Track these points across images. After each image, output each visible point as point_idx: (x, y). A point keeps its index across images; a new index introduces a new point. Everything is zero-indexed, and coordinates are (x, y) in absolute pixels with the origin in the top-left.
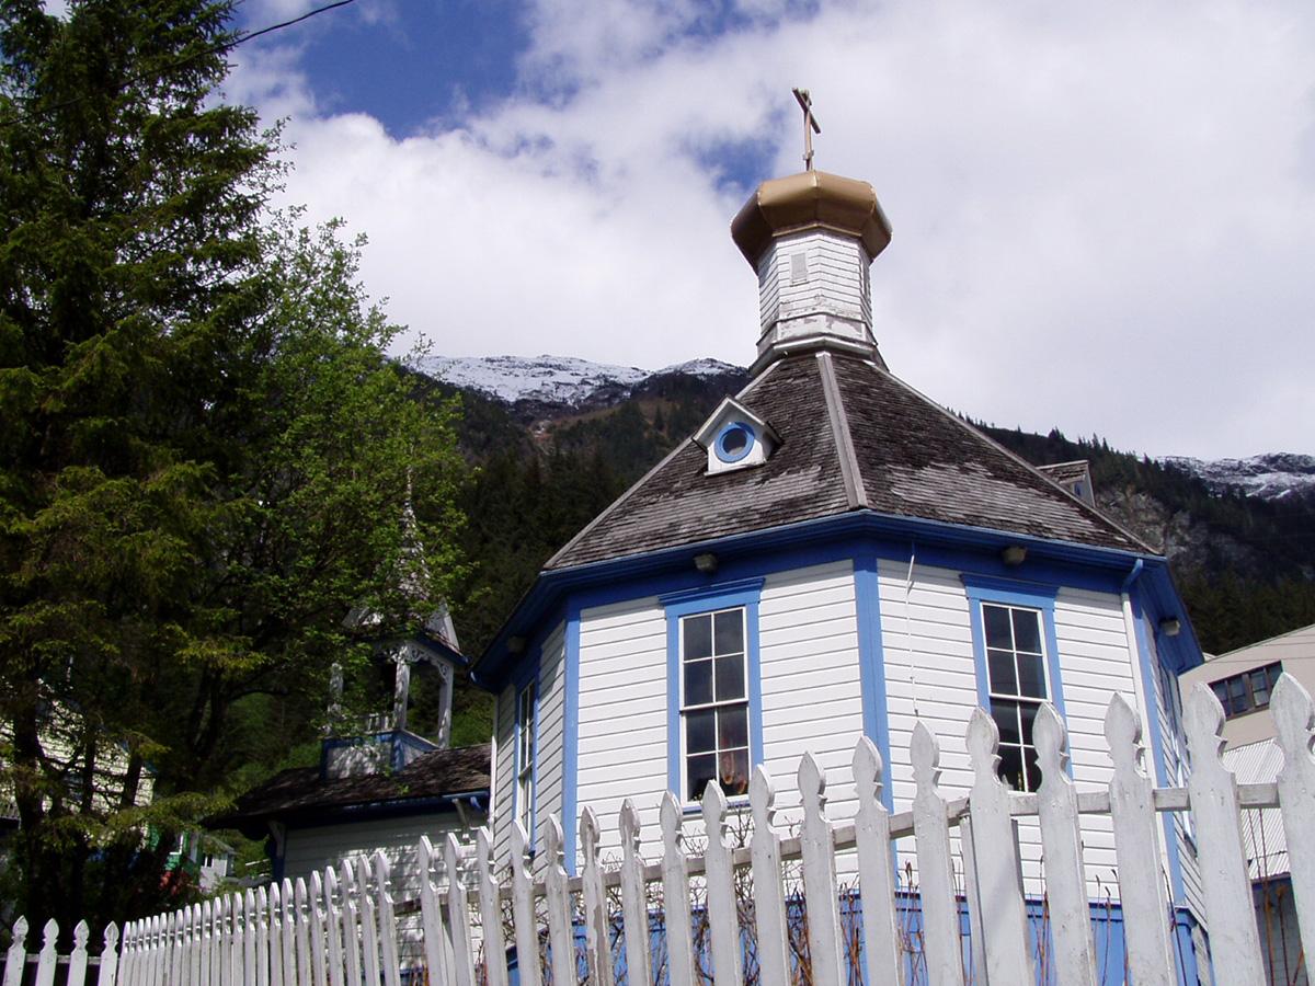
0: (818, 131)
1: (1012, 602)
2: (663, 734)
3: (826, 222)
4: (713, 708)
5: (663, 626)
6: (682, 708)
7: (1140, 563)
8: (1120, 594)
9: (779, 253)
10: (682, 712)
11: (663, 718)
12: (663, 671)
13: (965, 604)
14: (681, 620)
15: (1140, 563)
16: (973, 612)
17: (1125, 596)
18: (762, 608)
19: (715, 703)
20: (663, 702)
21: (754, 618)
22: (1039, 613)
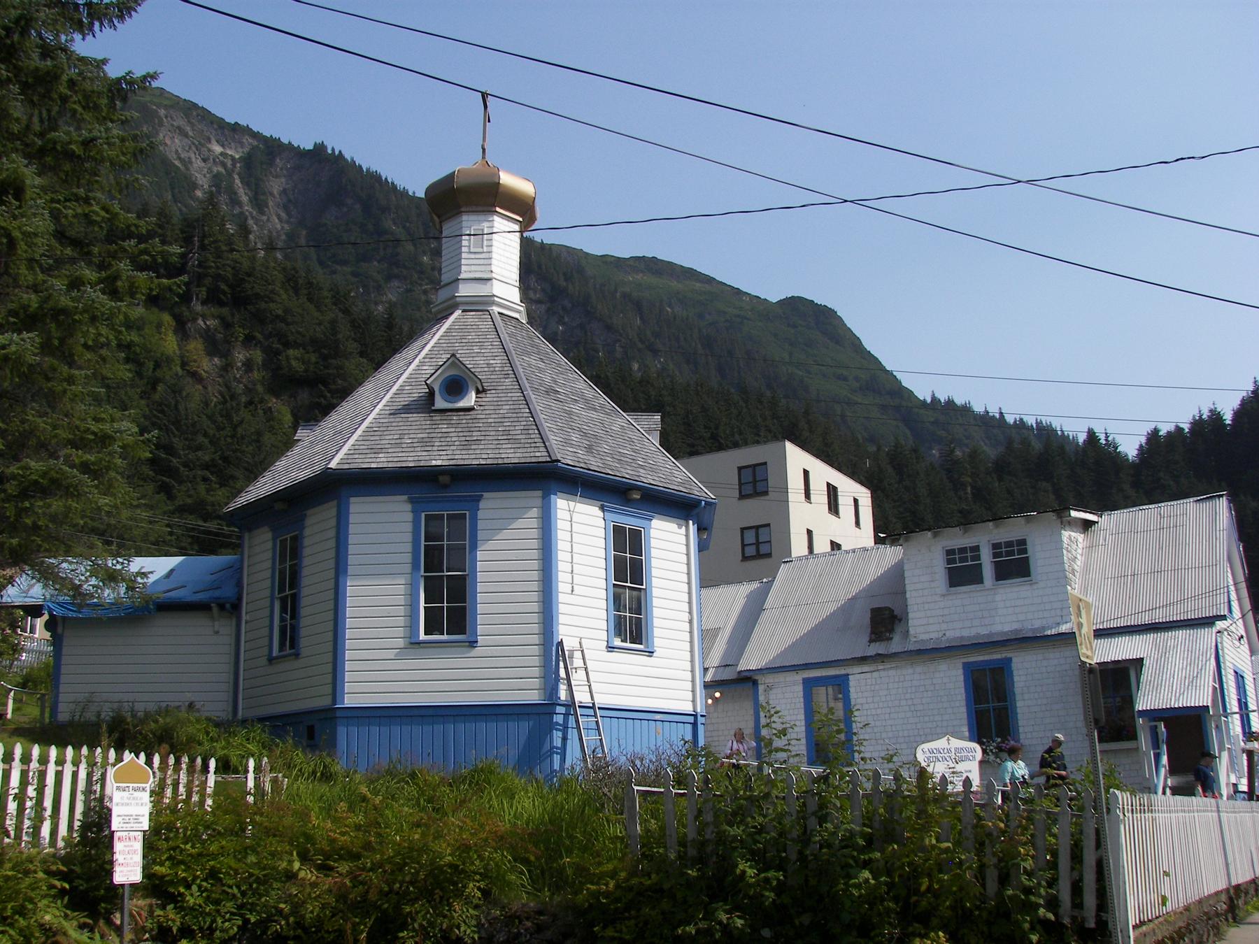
1: (629, 522)
5: (410, 517)
9: (464, 224)
12: (409, 547)
14: (423, 515)
18: (480, 514)
21: (474, 519)
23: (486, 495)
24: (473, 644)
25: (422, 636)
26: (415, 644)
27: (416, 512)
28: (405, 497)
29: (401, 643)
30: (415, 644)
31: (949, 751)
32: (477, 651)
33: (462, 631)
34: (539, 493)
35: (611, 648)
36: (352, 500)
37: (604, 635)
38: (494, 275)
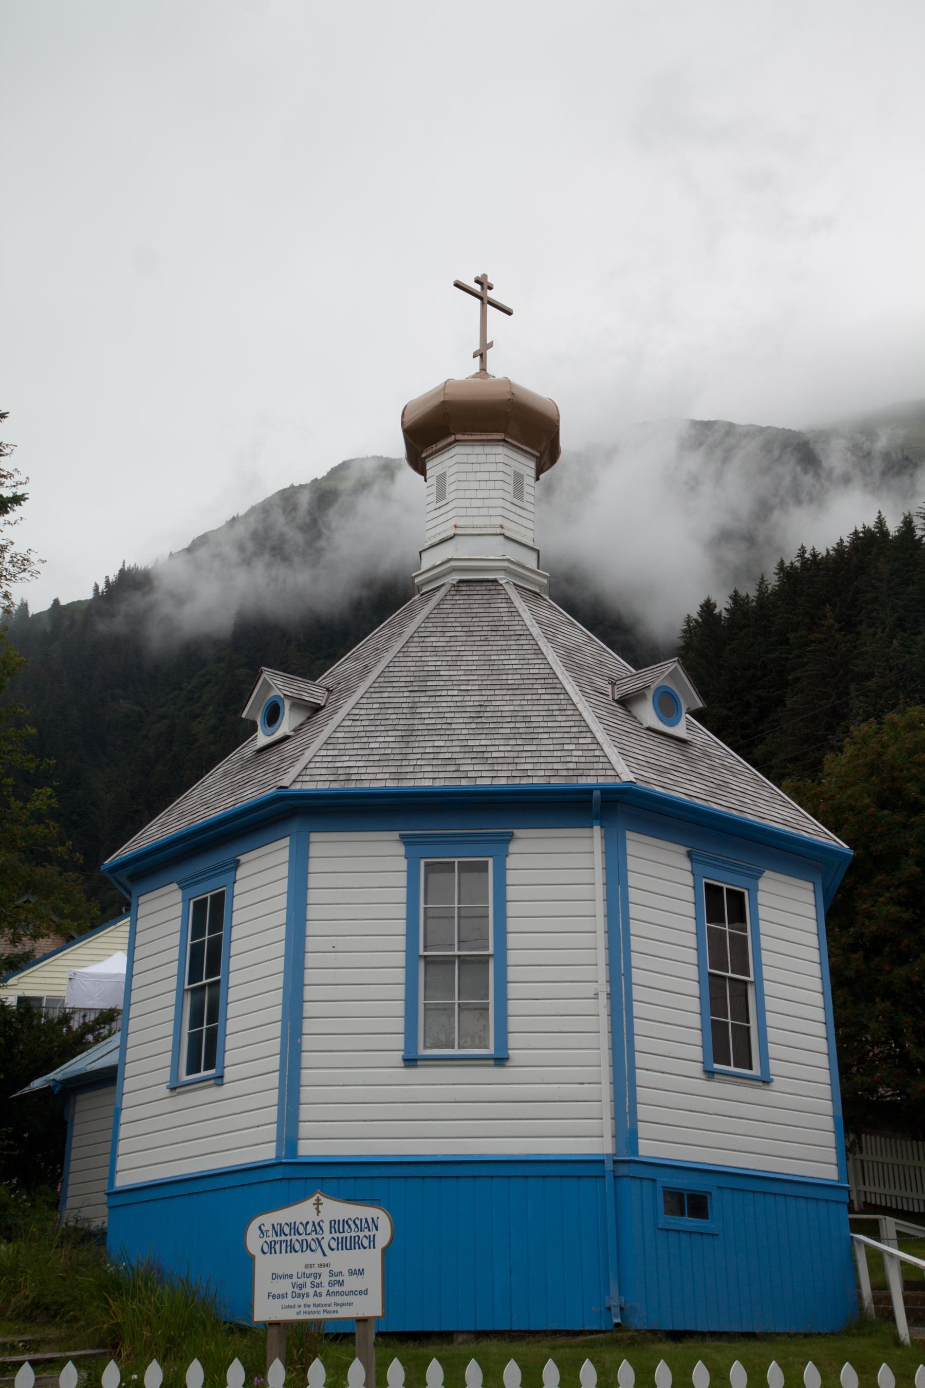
0: (509, 313)
2: (171, 1013)
3: (464, 432)
4: (203, 986)
6: (186, 987)
7: (597, 794)
8: (592, 827)
10: (188, 990)
11: (172, 998)
13: (403, 864)
15: (597, 794)
16: (412, 874)
17: (597, 831)
18: (238, 888)
19: (204, 981)
20: (173, 983)
22: (491, 861)
23: (243, 858)
24: (219, 1080)
25: (184, 1078)
26: (175, 1088)
27: (185, 901)
28: (174, 886)
29: (164, 1091)
30: (175, 1088)
31: (317, 1227)
32: (226, 1090)
33: (210, 1065)
34: (286, 841)
35: (410, 1061)
36: (142, 899)
37: (399, 1042)
38: (459, 531)
